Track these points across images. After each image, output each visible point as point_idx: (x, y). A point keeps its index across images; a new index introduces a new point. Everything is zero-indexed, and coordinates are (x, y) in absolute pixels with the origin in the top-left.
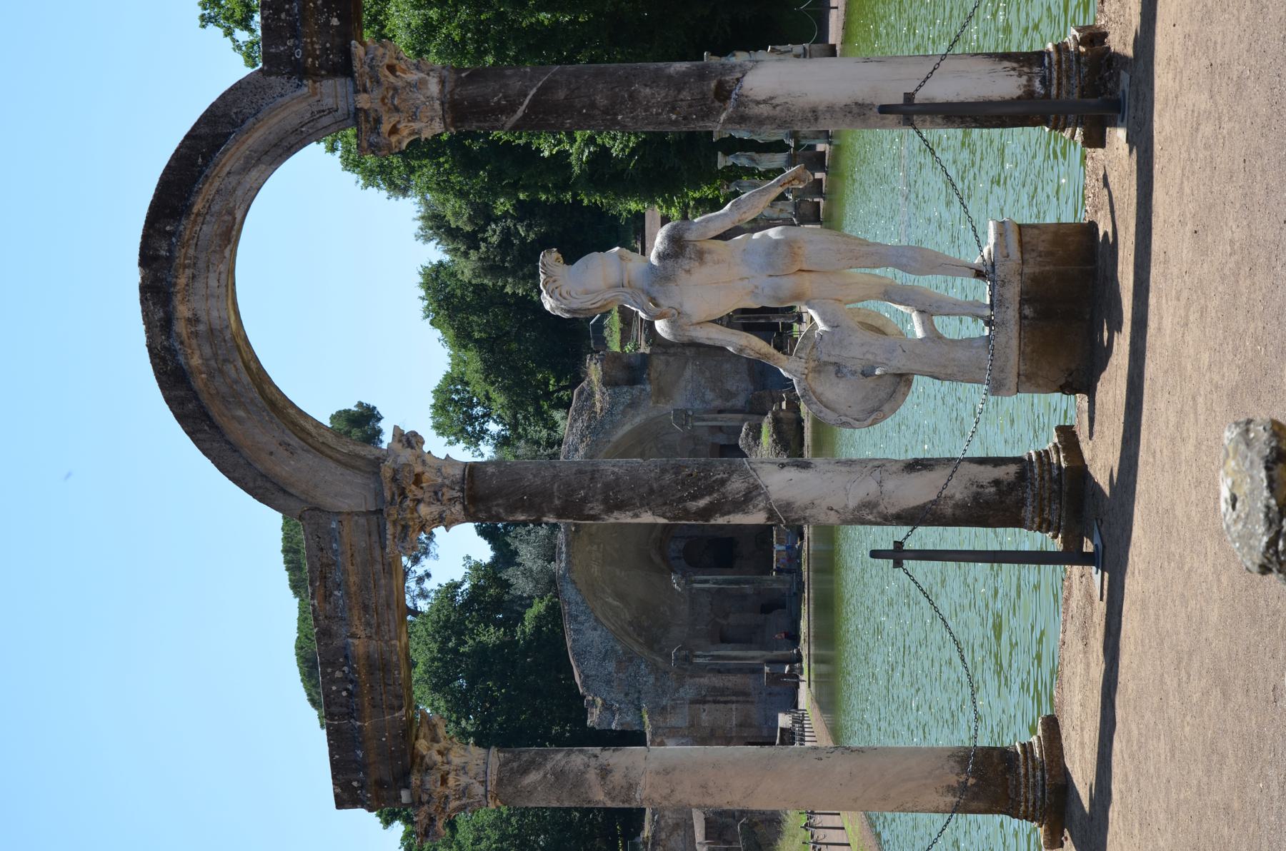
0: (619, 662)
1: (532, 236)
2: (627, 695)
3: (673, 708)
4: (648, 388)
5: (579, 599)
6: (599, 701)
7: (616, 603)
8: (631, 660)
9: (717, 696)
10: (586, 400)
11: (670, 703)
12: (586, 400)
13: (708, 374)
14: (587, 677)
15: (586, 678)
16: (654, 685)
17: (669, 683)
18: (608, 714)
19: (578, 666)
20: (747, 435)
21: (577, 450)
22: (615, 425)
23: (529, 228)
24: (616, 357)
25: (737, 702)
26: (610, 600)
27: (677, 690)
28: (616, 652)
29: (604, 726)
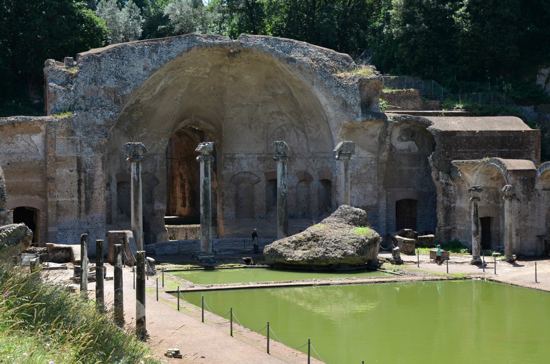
0: (115, 92)
1: (458, 20)
2: (83, 97)
3: (73, 142)
4: (359, 119)
5: (173, 54)
6: (74, 71)
7: (159, 88)
8: (117, 102)
9: (85, 183)
10: (344, 65)
11: (78, 139)
12: (344, 65)
13: (364, 171)
14: (99, 60)
15: (97, 59)
16: (94, 124)
17: (96, 138)
18: (62, 79)
19: (108, 52)
20: (356, 213)
21: (305, 55)
22: (328, 89)
23: (463, 16)
24: (377, 92)
25: (80, 202)
26: (162, 83)
27: (90, 145)
28: (124, 88)
29: (49, 75)
